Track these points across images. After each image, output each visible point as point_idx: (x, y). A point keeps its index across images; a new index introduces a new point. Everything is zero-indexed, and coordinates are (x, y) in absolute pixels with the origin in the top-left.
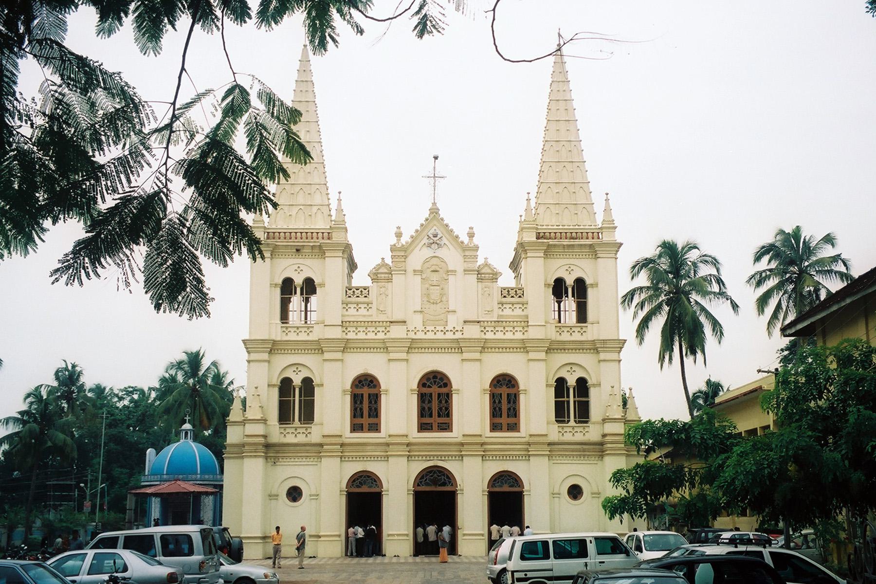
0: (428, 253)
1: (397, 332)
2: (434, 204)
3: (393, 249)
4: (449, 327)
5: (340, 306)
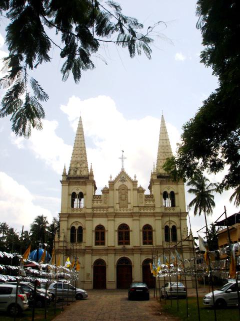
0: (120, 183)
1: (111, 210)
2: (123, 167)
3: (109, 182)
5: (91, 201)
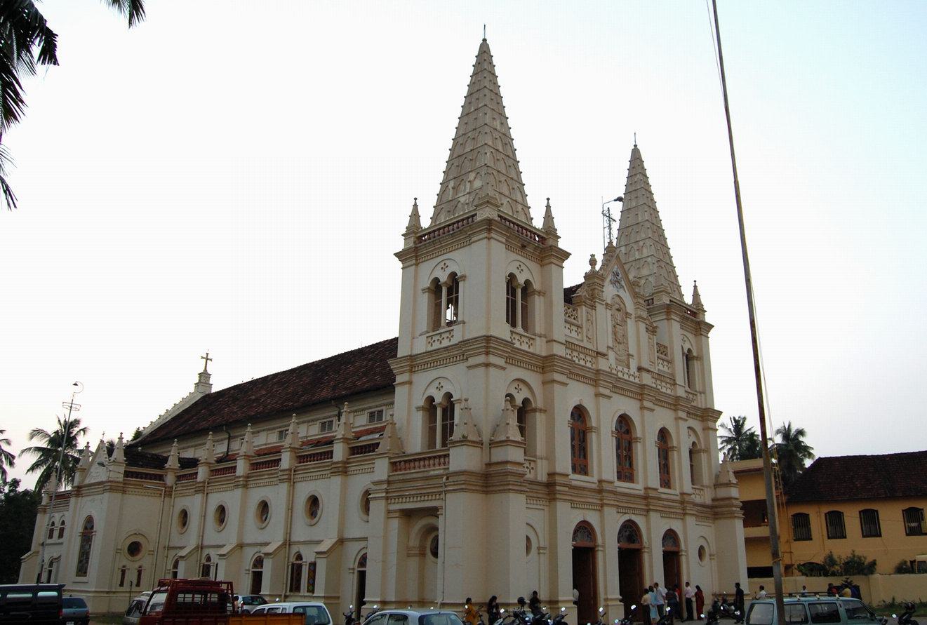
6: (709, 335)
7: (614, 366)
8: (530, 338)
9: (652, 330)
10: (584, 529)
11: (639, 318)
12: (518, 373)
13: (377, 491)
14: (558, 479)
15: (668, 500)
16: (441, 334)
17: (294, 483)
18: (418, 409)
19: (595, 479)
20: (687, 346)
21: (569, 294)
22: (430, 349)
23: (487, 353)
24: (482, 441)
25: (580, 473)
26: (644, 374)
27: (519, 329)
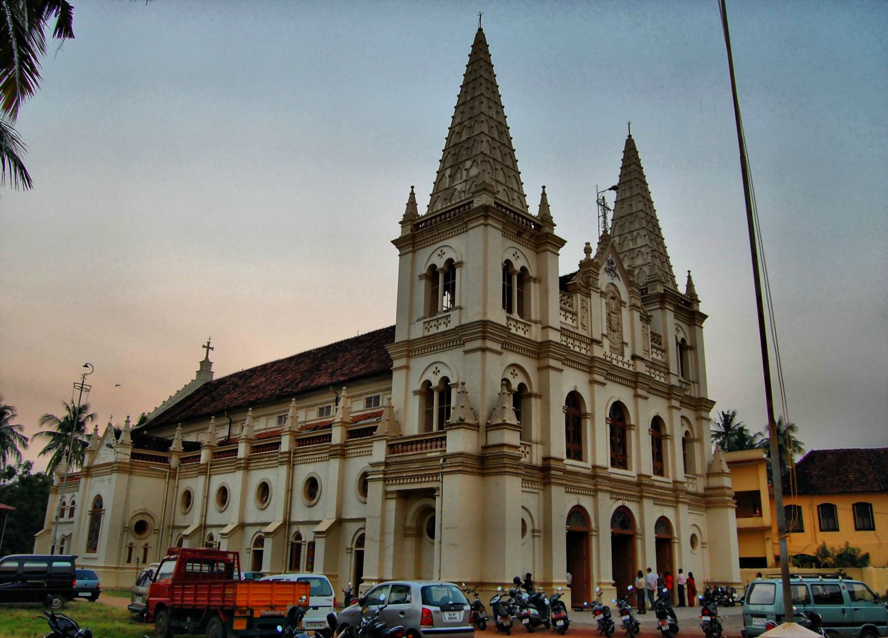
4: (626, 360)
6: (703, 325)
7: (608, 354)
8: (525, 325)
9: (646, 319)
10: (577, 513)
11: (633, 307)
12: (512, 358)
13: (374, 473)
14: (553, 463)
15: (661, 488)
16: (437, 320)
17: (293, 465)
18: (415, 393)
19: (589, 465)
20: (681, 336)
21: (565, 281)
22: (427, 334)
23: (484, 338)
24: (478, 424)
25: (574, 458)
26: (638, 363)
27: (515, 315)
